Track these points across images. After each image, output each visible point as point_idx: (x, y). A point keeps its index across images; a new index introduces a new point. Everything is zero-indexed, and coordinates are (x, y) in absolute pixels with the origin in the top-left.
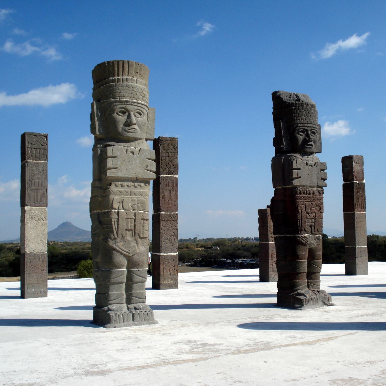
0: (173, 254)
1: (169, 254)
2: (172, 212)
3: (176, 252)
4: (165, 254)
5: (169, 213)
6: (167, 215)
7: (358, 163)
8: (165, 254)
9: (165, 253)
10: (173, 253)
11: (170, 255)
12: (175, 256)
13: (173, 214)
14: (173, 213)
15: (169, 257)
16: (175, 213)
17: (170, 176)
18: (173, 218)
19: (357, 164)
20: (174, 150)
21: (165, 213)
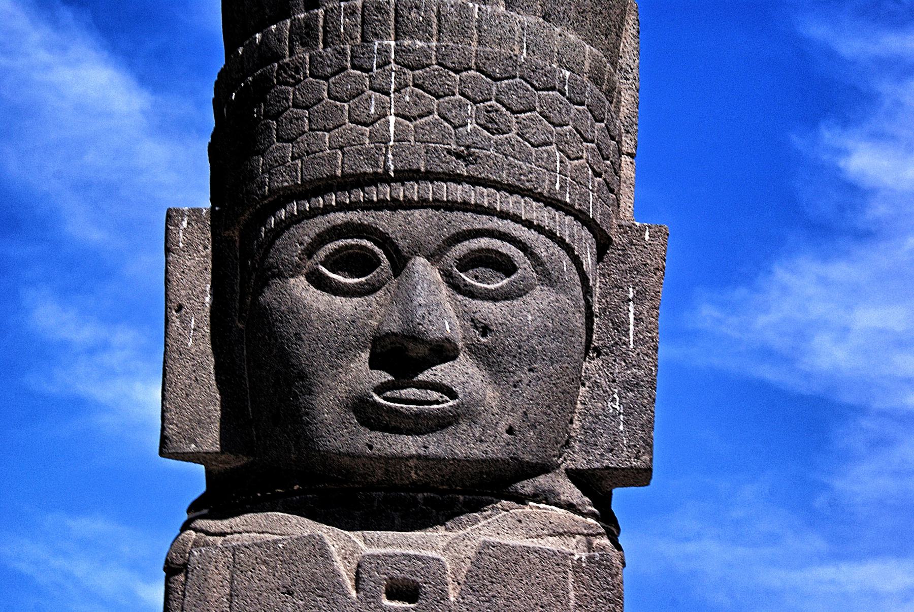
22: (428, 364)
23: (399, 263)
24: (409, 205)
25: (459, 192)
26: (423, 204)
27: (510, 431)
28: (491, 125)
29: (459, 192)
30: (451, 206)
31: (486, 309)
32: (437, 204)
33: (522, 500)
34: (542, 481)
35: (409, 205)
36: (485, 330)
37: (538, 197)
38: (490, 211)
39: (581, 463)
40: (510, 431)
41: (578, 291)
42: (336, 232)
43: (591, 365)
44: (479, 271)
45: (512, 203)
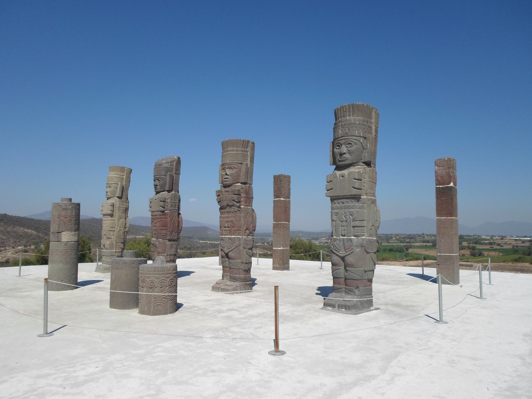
0: (279, 248)
4: (275, 248)
7: (442, 167)
8: (275, 248)
19: (441, 168)
20: (280, 182)
22: (342, 155)
23: (341, 146)
24: (342, 140)
25: (346, 138)
26: (343, 139)
27: (352, 160)
28: (349, 130)
29: (346, 138)
30: (345, 139)
31: (349, 149)
32: (344, 139)
33: (355, 166)
34: (357, 164)
35: (342, 140)
36: (349, 151)
37: (354, 136)
38: (349, 139)
39: (363, 161)
40: (352, 160)
41: (360, 144)
42: (336, 144)
43: (364, 151)
44: (349, 145)
45: (351, 137)
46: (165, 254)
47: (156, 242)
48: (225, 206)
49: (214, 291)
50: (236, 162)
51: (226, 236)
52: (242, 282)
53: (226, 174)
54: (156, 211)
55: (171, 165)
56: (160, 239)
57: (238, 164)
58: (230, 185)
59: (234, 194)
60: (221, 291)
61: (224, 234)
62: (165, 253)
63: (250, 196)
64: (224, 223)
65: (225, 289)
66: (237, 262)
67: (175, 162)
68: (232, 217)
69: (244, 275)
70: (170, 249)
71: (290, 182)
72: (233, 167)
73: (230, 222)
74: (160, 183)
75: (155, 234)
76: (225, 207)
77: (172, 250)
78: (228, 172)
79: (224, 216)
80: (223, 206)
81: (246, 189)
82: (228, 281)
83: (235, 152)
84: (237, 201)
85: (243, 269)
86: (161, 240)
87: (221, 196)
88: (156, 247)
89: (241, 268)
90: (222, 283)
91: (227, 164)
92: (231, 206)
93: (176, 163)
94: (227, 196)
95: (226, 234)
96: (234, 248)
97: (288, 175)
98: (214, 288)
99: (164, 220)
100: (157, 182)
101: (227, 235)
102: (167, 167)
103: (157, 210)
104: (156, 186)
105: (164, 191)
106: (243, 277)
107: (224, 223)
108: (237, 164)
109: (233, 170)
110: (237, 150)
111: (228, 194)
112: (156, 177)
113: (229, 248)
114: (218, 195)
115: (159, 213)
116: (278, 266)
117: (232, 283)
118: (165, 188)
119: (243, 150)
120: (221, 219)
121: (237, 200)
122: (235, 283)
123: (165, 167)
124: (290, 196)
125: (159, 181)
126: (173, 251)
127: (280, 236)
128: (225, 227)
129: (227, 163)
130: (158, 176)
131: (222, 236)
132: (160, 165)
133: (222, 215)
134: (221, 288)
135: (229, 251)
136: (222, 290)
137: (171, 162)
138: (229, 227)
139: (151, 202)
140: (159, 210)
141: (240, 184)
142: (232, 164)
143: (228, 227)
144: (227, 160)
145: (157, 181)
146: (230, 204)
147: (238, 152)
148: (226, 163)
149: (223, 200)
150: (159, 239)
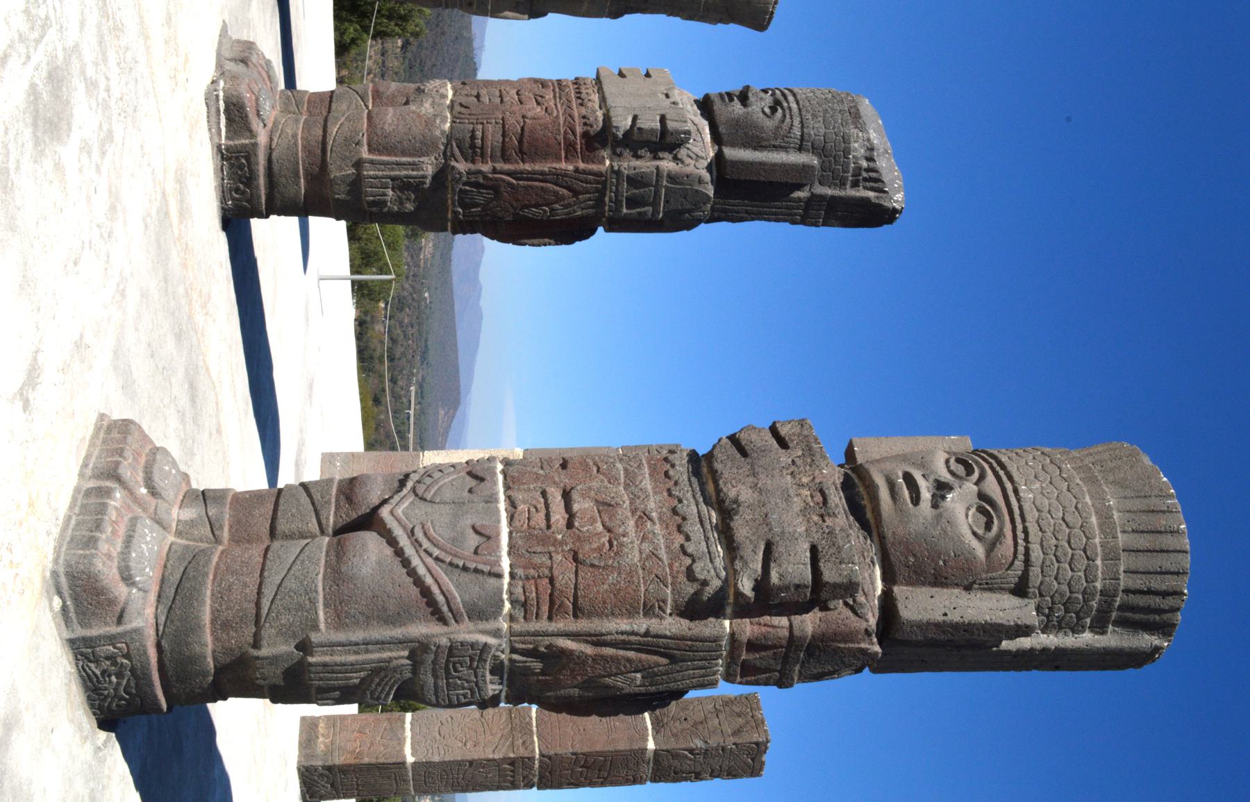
1: (408, 734)
2: (538, 737)
3: (413, 755)
4: (408, 726)
5: (535, 729)
6: (530, 724)
8: (408, 726)
9: (411, 723)
10: (413, 748)
11: (405, 739)
12: (401, 751)
13: (533, 742)
14: (536, 739)
15: (400, 736)
16: (537, 745)
17: (650, 726)
18: (521, 741)
20: (730, 731)
21: (534, 719)
46: (366, 147)
47: (433, 104)
48: (718, 491)
49: (95, 436)
50: (1036, 553)
51: (502, 505)
52: (159, 646)
53: (942, 488)
54: (603, 99)
55: (858, 170)
56: (453, 122)
57: (1019, 564)
58: (869, 515)
59: (814, 550)
60: (88, 493)
61: (519, 496)
62: (371, 150)
63: (797, 668)
64: (595, 484)
65: (98, 526)
66: (313, 602)
67: (871, 194)
68: (647, 547)
69: (215, 659)
70: (393, 179)
71: (732, 774)
72: (1000, 534)
73: (609, 531)
74: (761, 115)
75: (478, 97)
76: (710, 488)
77: (390, 193)
78: (960, 503)
79: (647, 484)
80: (713, 472)
81: (850, 636)
82: (171, 538)
83: (1097, 540)
84: (774, 578)
85: (256, 644)
86: (448, 125)
87: (784, 458)
88: (407, 103)
89: (268, 632)
90: (153, 492)
91: (1009, 486)
92: (726, 534)
93: (866, 201)
94: (788, 499)
95: (522, 507)
96: (422, 571)
97: (763, 763)
98: (115, 435)
99: (561, 138)
100: (760, 105)
101: (511, 519)
102: (847, 152)
103: (610, 101)
104: (744, 97)
105: (717, 138)
106: (197, 648)
107: (595, 484)
108: (1021, 557)
109: (980, 532)
110: (1111, 556)
111: (805, 511)
112: (791, 98)
113: (419, 534)
114: (784, 431)
115: (594, 111)
116: (321, 744)
117: (148, 573)
118: (733, 145)
119: (1115, 596)
120: (619, 466)
121: (781, 576)
122: (153, 597)
123: (846, 139)
124: (666, 781)
125: (767, 110)
126: (385, 195)
127: (468, 745)
128: (567, 496)
129: (1016, 491)
130: (794, 106)
131: (500, 478)
132: (856, 116)
133: (646, 470)
134: (107, 493)
135: (399, 533)
136: (93, 500)
137: (873, 175)
138: (570, 525)
139: (648, 75)
140: (612, 114)
141: (879, 592)
142: (1020, 527)
143: (571, 516)
144: (1038, 485)
145: (768, 99)
146: (742, 529)
147: (1099, 562)
148: (1010, 478)
149: (755, 475)
150: (453, 117)
